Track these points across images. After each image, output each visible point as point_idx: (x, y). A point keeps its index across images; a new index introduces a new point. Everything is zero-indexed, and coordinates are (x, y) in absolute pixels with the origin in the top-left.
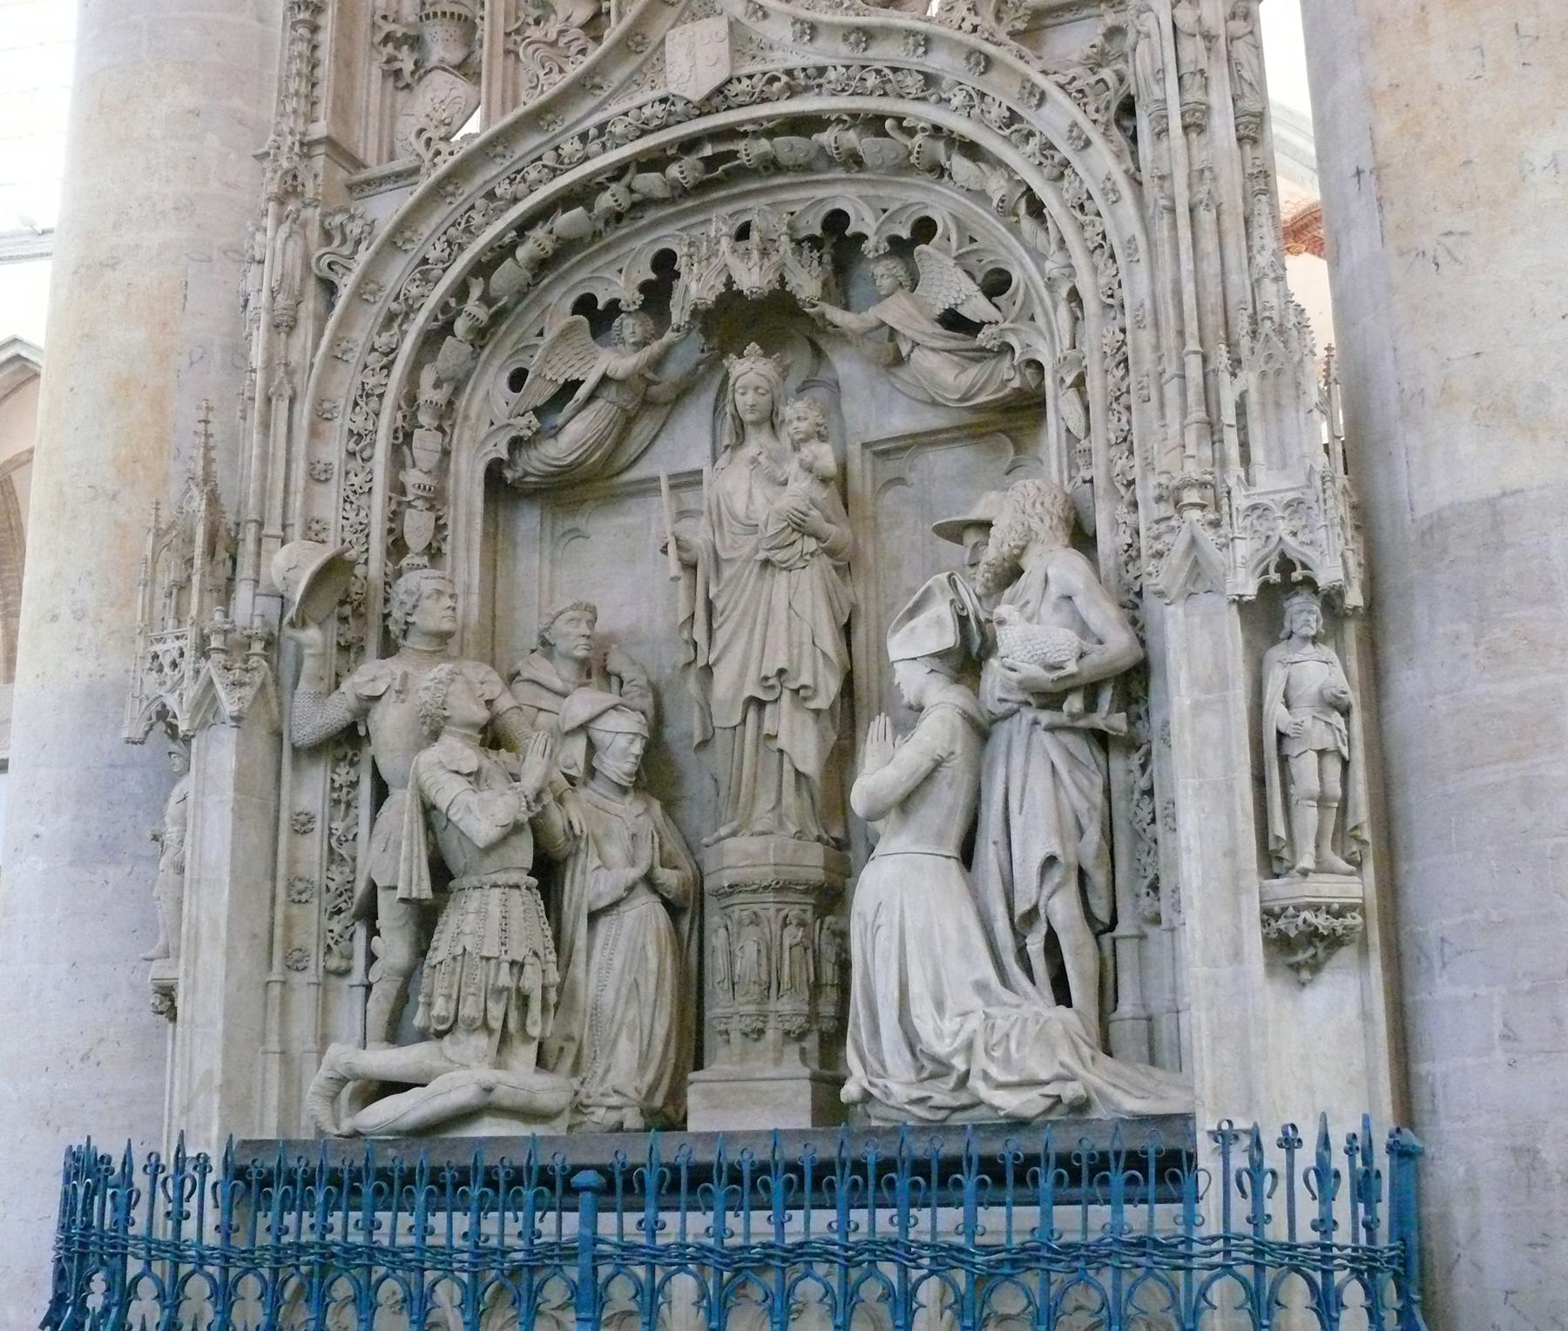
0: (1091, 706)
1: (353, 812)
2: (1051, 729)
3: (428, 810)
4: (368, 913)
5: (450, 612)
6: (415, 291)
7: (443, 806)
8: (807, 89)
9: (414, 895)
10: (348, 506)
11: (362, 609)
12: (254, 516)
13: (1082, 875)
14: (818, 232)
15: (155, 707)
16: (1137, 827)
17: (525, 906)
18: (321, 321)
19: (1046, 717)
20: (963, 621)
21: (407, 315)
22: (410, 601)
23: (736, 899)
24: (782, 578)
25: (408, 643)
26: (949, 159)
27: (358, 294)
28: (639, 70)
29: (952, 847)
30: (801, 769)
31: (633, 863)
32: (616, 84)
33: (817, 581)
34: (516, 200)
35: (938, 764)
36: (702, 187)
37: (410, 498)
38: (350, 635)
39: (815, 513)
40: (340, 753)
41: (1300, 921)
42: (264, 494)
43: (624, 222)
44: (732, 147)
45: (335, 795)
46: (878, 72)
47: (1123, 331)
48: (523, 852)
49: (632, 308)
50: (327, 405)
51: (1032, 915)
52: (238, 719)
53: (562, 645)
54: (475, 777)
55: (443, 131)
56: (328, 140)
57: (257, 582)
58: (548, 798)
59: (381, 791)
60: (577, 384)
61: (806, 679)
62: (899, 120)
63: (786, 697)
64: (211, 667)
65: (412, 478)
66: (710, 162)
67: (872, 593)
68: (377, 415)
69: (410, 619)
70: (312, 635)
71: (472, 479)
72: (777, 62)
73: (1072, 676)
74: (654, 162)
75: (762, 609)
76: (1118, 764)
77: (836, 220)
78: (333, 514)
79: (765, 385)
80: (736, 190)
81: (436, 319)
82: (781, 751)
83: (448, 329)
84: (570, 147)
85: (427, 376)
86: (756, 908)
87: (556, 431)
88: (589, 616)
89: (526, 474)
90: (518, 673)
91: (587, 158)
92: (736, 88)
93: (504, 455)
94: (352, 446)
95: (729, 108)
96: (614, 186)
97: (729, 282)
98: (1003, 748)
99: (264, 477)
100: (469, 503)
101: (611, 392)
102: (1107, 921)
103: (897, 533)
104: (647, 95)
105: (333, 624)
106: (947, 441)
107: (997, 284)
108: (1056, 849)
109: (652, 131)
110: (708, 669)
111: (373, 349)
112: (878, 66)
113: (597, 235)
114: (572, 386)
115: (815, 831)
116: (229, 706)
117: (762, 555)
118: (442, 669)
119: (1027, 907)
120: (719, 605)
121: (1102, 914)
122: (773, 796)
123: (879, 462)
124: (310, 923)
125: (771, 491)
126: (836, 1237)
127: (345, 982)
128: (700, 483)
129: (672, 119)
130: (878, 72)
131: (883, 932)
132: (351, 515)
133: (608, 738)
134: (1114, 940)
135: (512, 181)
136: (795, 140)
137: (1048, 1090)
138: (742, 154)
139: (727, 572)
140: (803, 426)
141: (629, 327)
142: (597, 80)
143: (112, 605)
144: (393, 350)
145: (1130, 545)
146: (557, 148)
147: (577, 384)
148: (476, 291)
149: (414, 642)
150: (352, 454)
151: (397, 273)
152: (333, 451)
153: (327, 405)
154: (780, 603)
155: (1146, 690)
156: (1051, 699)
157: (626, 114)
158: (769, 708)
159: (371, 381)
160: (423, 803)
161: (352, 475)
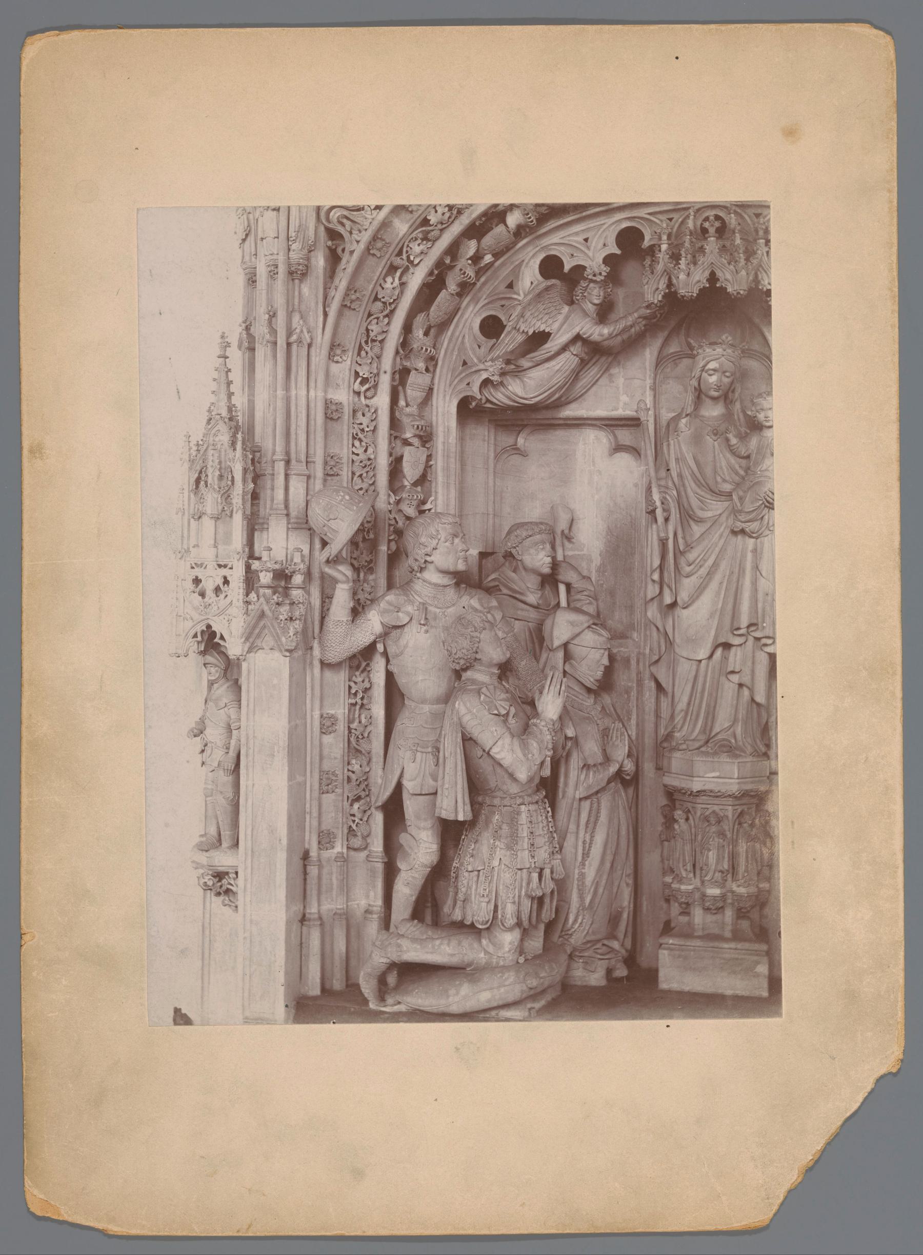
4: (394, 810)
6: (416, 248)
10: (357, 443)
21: (407, 269)
27: (368, 249)
37: (408, 435)
45: (353, 701)
68: (379, 357)
78: (345, 451)
86: (716, 808)
87: (518, 372)
94: (357, 386)
101: (577, 348)
132: (360, 451)
150: (358, 394)
161: (359, 414)
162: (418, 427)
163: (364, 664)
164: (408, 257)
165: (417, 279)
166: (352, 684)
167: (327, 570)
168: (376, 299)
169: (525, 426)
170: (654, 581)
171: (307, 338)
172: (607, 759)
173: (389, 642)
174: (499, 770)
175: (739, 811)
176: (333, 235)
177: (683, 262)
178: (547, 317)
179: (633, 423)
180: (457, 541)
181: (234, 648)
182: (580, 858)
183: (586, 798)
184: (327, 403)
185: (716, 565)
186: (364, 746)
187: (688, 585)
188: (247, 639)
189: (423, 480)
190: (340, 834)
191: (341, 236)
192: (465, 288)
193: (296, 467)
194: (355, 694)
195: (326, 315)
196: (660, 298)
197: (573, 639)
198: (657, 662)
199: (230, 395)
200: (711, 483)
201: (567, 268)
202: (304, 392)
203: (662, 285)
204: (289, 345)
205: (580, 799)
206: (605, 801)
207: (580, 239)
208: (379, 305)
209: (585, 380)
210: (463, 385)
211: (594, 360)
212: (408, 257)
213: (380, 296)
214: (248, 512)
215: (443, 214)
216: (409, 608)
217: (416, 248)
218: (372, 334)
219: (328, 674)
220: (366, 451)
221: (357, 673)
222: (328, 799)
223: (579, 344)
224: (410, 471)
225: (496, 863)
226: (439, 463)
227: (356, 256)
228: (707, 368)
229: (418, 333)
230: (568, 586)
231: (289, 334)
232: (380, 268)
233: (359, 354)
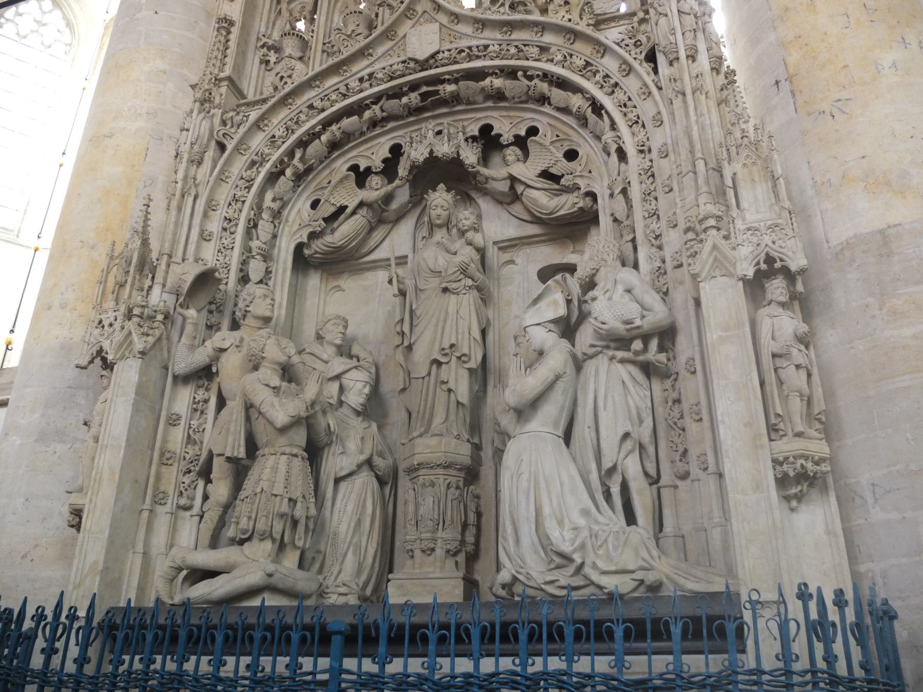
0: (646, 349)
1: (204, 416)
2: (622, 361)
3: (249, 407)
5: (270, 307)
7: (257, 403)
8: (478, 57)
9: (235, 454)
11: (222, 308)
12: (167, 251)
13: (641, 447)
14: (477, 133)
15: (96, 348)
16: (670, 422)
17: (299, 466)
19: (620, 354)
20: (569, 302)
21: (261, 164)
22: (249, 299)
24: (453, 298)
25: (247, 321)
26: (550, 91)
27: (237, 149)
28: (391, 48)
29: (560, 433)
30: (460, 400)
31: (362, 452)
32: (380, 54)
33: (472, 301)
34: (323, 110)
35: (558, 378)
36: (419, 110)
37: (254, 254)
38: (213, 320)
39: (472, 265)
40: (201, 382)
41: (798, 466)
42: (174, 242)
43: (377, 128)
44: (436, 88)
46: (516, 46)
47: (651, 161)
48: (300, 436)
49: (379, 170)
50: (214, 203)
51: (612, 470)
52: (143, 353)
53: (328, 337)
54: (276, 389)
55: (290, 72)
56: (229, 79)
57: (164, 286)
58: (317, 408)
59: (222, 403)
60: (346, 207)
61: (466, 351)
62: (525, 70)
63: (454, 359)
64: (131, 325)
65: (255, 244)
66: (427, 93)
67: (496, 316)
69: (248, 309)
70: (191, 313)
71: (287, 251)
72: (464, 43)
73: (638, 327)
74: (395, 93)
75: (443, 314)
76: (657, 386)
77: (486, 129)
79: (446, 205)
80: (436, 112)
81: (276, 167)
82: (450, 390)
83: (282, 173)
84: (354, 84)
85: (269, 196)
87: (333, 231)
88: (344, 324)
89: (316, 252)
90: (304, 350)
91: (361, 91)
92: (440, 56)
93: (305, 240)
94: (225, 225)
95: (437, 67)
96: (374, 107)
98: (593, 373)
99: (175, 234)
100: (285, 263)
101: (364, 211)
102: (655, 476)
103: (510, 288)
104: (395, 60)
105: (205, 313)
106: (537, 242)
107: (571, 155)
108: (629, 428)
109: (396, 78)
110: (410, 348)
111: (242, 178)
112: (516, 43)
113: (362, 134)
114: (342, 209)
115: (466, 436)
116: (139, 344)
117: (444, 285)
118: (264, 332)
119: (610, 465)
120: (418, 313)
121: (652, 472)
122: (444, 416)
123: (501, 253)
125: (448, 257)
126: (519, 669)
128: (406, 263)
129: (407, 72)
130: (516, 46)
131: (525, 477)
132: (221, 259)
133: (351, 384)
134: (659, 489)
135: (322, 100)
136: (471, 83)
137: (634, 576)
138: (441, 92)
139: (423, 296)
140: (467, 223)
141: (375, 181)
142: (371, 51)
143: (83, 302)
144: (252, 180)
145: (659, 268)
146: (346, 85)
147: (346, 207)
148: (298, 155)
149: (249, 321)
150: (225, 229)
151: (258, 141)
152: (214, 226)
153: (214, 203)
154: (452, 309)
155: (673, 344)
156: (623, 342)
157: (384, 69)
158: (444, 366)
160: (246, 404)
161: (223, 239)
163: (206, 383)
192: (299, 177)
224: (255, 275)
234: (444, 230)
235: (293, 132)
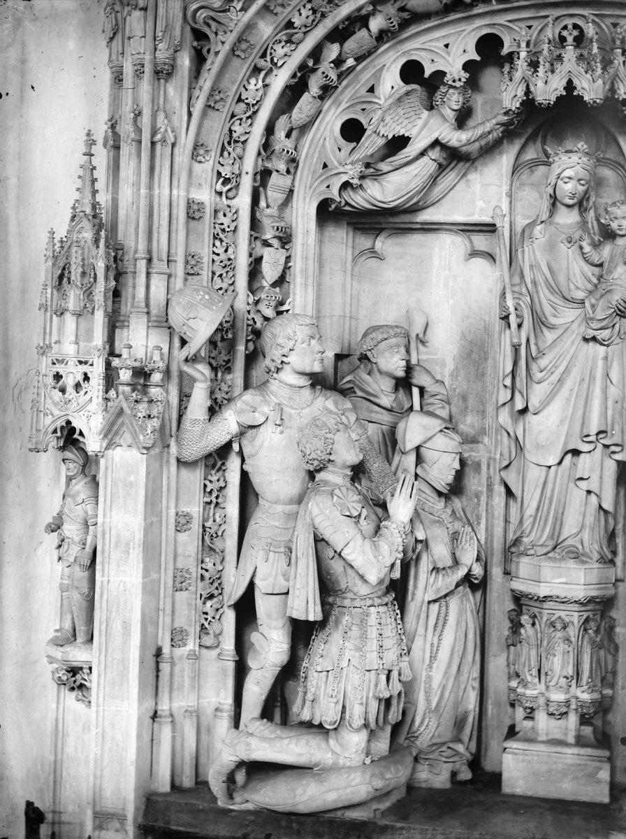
6: (280, 51)
10: (218, 243)
18: (197, 72)
21: (271, 70)
23: (546, 605)
27: (233, 50)
45: (208, 500)
63: (600, 447)
78: (206, 250)
86: (562, 614)
87: (378, 175)
94: (219, 187)
97: (570, 86)
101: (436, 153)
114: (398, 143)
117: (591, 333)
124: (186, 608)
127: (214, 653)
132: (220, 250)
139: (549, 336)
150: (220, 194)
159: (236, 127)
161: (220, 215)
162: (278, 229)
163: (219, 463)
164: (272, 59)
165: (280, 80)
166: (207, 483)
167: (186, 368)
168: (240, 100)
169: (381, 230)
170: (505, 386)
171: (171, 139)
172: (456, 562)
173: (245, 442)
174: (350, 571)
175: (585, 617)
176: (199, 35)
177: (541, 69)
178: (406, 122)
179: (489, 228)
180: (313, 342)
181: (93, 444)
182: (427, 661)
183: (435, 601)
184: (189, 203)
185: (567, 371)
186: (218, 544)
187: (537, 394)
188: (105, 436)
189: (281, 281)
190: (193, 630)
191: (206, 37)
192: (327, 90)
193: (159, 266)
194: (210, 493)
195: (190, 114)
196: (518, 105)
197: (424, 442)
198: (507, 467)
199: (95, 193)
200: (564, 289)
201: (427, 74)
202: (167, 191)
203: (520, 92)
204: (153, 144)
205: (429, 602)
206: (454, 603)
207: (441, 45)
208: (242, 106)
209: (442, 186)
210: (323, 187)
211: (452, 165)
212: (272, 59)
213: (243, 98)
214: (110, 309)
215: (307, 17)
216: (266, 409)
217: (280, 51)
218: (235, 135)
219: (185, 472)
220: (226, 251)
221: (213, 472)
222: (182, 596)
223: (438, 149)
224: (270, 272)
225: (344, 664)
226: (297, 264)
227: (221, 57)
228: (562, 176)
229: (280, 133)
230: (422, 390)
231: (154, 132)
232: (243, 69)
233: (222, 155)
234: (576, 210)
235: (323, 15)
